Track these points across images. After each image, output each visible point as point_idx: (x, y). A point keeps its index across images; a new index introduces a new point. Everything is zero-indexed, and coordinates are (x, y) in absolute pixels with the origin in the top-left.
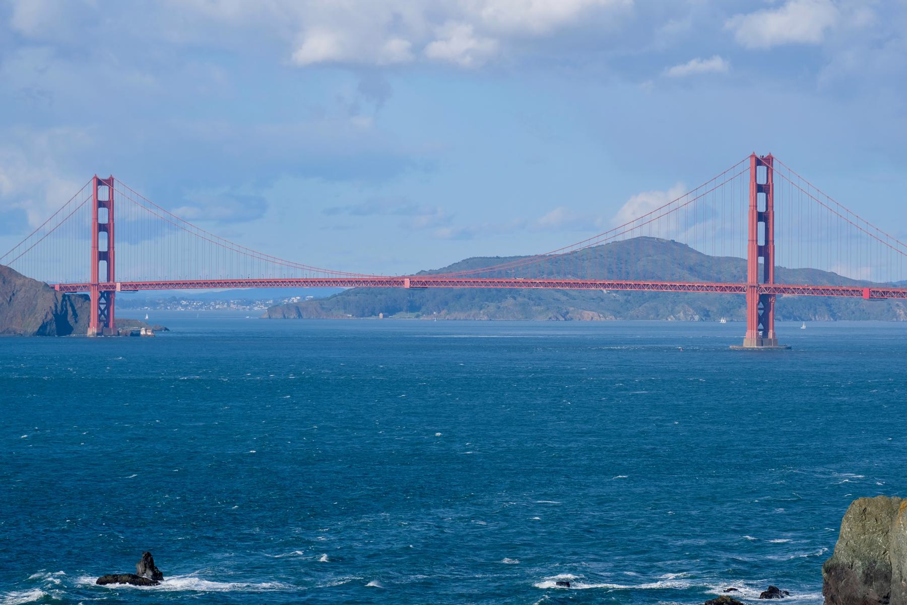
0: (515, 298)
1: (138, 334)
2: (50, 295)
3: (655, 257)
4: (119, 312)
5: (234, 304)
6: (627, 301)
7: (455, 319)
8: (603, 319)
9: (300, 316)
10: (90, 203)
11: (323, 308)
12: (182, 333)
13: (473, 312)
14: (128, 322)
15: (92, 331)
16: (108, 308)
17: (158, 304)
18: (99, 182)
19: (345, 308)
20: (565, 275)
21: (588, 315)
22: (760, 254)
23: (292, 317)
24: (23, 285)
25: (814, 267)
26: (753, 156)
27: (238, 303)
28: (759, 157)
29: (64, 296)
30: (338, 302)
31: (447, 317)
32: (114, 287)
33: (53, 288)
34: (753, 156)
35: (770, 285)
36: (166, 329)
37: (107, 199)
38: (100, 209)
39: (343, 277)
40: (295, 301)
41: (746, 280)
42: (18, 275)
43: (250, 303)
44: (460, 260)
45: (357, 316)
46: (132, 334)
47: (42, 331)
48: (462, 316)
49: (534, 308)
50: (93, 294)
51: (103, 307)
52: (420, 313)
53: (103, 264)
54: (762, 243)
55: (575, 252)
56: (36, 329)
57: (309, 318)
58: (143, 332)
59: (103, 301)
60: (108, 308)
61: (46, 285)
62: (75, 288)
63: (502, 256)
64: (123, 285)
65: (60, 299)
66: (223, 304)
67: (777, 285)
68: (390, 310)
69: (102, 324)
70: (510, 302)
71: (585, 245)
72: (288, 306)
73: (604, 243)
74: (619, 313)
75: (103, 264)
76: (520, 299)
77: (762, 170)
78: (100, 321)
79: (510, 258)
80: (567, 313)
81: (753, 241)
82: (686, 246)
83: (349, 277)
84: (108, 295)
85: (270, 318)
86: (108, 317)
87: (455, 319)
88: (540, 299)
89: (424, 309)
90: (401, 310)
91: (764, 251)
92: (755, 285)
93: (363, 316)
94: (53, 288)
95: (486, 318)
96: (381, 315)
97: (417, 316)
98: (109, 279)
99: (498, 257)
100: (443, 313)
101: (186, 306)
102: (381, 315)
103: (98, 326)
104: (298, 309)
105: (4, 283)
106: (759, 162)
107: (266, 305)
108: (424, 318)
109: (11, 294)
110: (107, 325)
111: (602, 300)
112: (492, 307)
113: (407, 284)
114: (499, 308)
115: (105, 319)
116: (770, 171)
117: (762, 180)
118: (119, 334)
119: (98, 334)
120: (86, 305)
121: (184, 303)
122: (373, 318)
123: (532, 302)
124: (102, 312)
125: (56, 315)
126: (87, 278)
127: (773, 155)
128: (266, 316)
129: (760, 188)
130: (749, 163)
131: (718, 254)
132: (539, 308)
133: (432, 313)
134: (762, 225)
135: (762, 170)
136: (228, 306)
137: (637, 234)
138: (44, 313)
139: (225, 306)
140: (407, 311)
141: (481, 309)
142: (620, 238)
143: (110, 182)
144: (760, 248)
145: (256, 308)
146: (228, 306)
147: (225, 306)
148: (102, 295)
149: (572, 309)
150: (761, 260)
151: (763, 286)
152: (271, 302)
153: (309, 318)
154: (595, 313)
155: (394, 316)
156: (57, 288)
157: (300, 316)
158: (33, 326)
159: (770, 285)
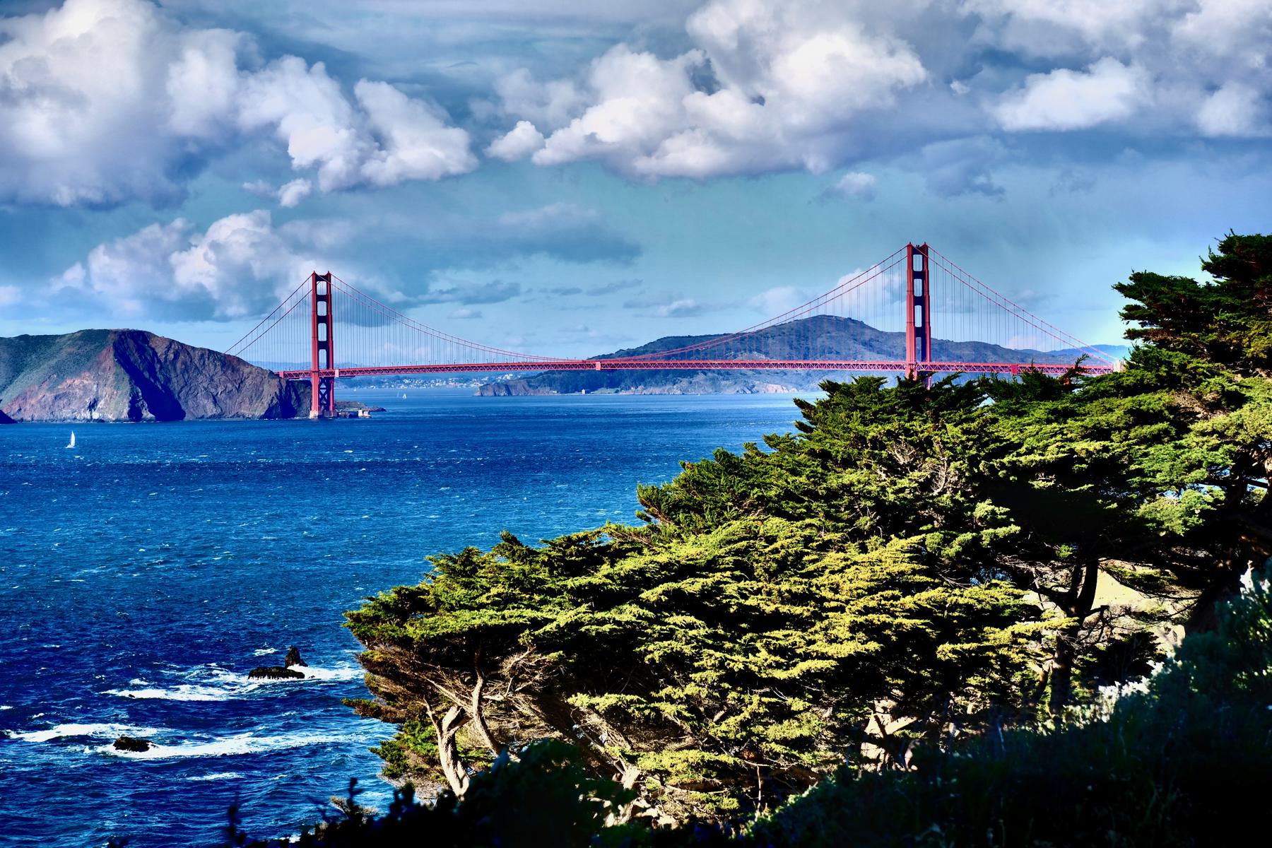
0: (705, 374)
1: (356, 415)
2: (275, 382)
3: (834, 334)
4: (340, 392)
5: (452, 381)
6: (809, 375)
7: (651, 394)
8: (786, 391)
9: (509, 393)
10: (310, 298)
11: (530, 386)
12: (403, 413)
13: (668, 387)
14: (349, 404)
15: (314, 414)
16: (328, 392)
17: (383, 382)
18: (317, 278)
19: (550, 386)
20: (751, 351)
21: (772, 388)
22: (917, 335)
23: (502, 394)
24: (251, 373)
25: (976, 340)
26: (910, 246)
27: (456, 381)
28: (915, 246)
29: (288, 382)
30: (544, 380)
31: (644, 392)
32: (334, 374)
33: (278, 375)
34: (908, 246)
35: (928, 363)
36: (383, 410)
37: (325, 293)
38: (319, 303)
39: (540, 361)
40: (508, 378)
41: (904, 357)
42: (245, 364)
43: (467, 380)
44: (655, 340)
45: (562, 393)
46: (351, 416)
47: (269, 414)
48: (657, 390)
49: (723, 383)
50: (314, 381)
51: (323, 391)
52: (619, 389)
53: (323, 353)
54: (919, 324)
55: (761, 331)
56: (263, 413)
57: (518, 395)
58: (360, 414)
59: (324, 386)
60: (328, 392)
61: (271, 373)
62: (297, 375)
63: (693, 335)
64: (341, 372)
65: (284, 384)
66: (442, 382)
67: (934, 363)
68: (592, 387)
69: (323, 407)
70: (701, 377)
71: (768, 325)
72: (498, 385)
73: (792, 320)
74: (801, 385)
75: (323, 353)
76: (710, 374)
77: (918, 259)
78: (320, 404)
79: (701, 336)
80: (754, 386)
81: (911, 323)
82: (862, 323)
83: (546, 361)
84: (328, 381)
85: (482, 395)
86: (328, 401)
87: (651, 394)
88: (728, 374)
89: (623, 385)
90: (601, 386)
91: (922, 332)
92: (914, 363)
93: (567, 392)
94: (278, 375)
95: (679, 392)
96: (583, 391)
97: (617, 392)
98: (328, 367)
99: (689, 336)
100: (640, 388)
101: (408, 384)
102: (583, 391)
103: (319, 409)
104: (508, 387)
105: (233, 371)
106: (913, 250)
107: (482, 382)
108: (623, 393)
109: (239, 381)
110: (327, 408)
111: (785, 374)
112: (685, 382)
113: (598, 367)
114: (691, 383)
115: (325, 402)
116: (925, 260)
117: (918, 267)
118: (338, 416)
119: (319, 416)
120: (308, 390)
121: (407, 381)
122: (577, 394)
123: (721, 377)
124: (323, 396)
125: (280, 398)
126: (311, 368)
127: (927, 244)
128: (478, 394)
129: (916, 275)
130: (905, 252)
131: (888, 330)
132: (727, 382)
133: (630, 388)
134: (918, 308)
135: (918, 259)
136: (447, 383)
137: (814, 314)
138: (270, 398)
139: (444, 383)
140: (607, 387)
141: (674, 384)
142: (799, 318)
143: (327, 278)
144: (917, 329)
145: (472, 385)
146: (447, 383)
147: (444, 383)
148: (322, 381)
149: (757, 382)
150: (919, 339)
151: (920, 364)
152: (486, 379)
153: (518, 395)
154: (779, 387)
155: (596, 392)
156: (281, 375)
157: (509, 393)
158: (260, 410)
159: (928, 363)
